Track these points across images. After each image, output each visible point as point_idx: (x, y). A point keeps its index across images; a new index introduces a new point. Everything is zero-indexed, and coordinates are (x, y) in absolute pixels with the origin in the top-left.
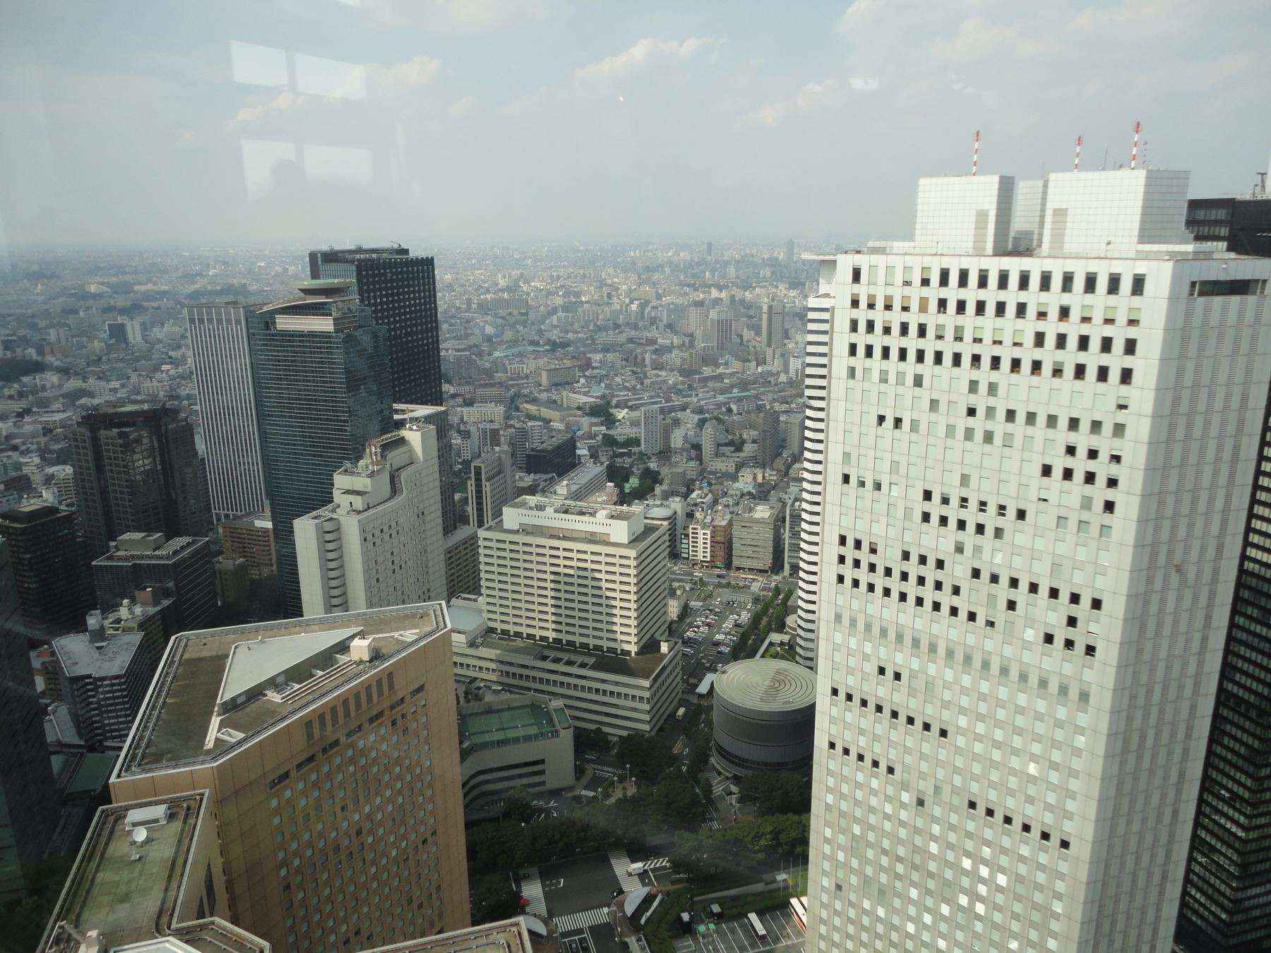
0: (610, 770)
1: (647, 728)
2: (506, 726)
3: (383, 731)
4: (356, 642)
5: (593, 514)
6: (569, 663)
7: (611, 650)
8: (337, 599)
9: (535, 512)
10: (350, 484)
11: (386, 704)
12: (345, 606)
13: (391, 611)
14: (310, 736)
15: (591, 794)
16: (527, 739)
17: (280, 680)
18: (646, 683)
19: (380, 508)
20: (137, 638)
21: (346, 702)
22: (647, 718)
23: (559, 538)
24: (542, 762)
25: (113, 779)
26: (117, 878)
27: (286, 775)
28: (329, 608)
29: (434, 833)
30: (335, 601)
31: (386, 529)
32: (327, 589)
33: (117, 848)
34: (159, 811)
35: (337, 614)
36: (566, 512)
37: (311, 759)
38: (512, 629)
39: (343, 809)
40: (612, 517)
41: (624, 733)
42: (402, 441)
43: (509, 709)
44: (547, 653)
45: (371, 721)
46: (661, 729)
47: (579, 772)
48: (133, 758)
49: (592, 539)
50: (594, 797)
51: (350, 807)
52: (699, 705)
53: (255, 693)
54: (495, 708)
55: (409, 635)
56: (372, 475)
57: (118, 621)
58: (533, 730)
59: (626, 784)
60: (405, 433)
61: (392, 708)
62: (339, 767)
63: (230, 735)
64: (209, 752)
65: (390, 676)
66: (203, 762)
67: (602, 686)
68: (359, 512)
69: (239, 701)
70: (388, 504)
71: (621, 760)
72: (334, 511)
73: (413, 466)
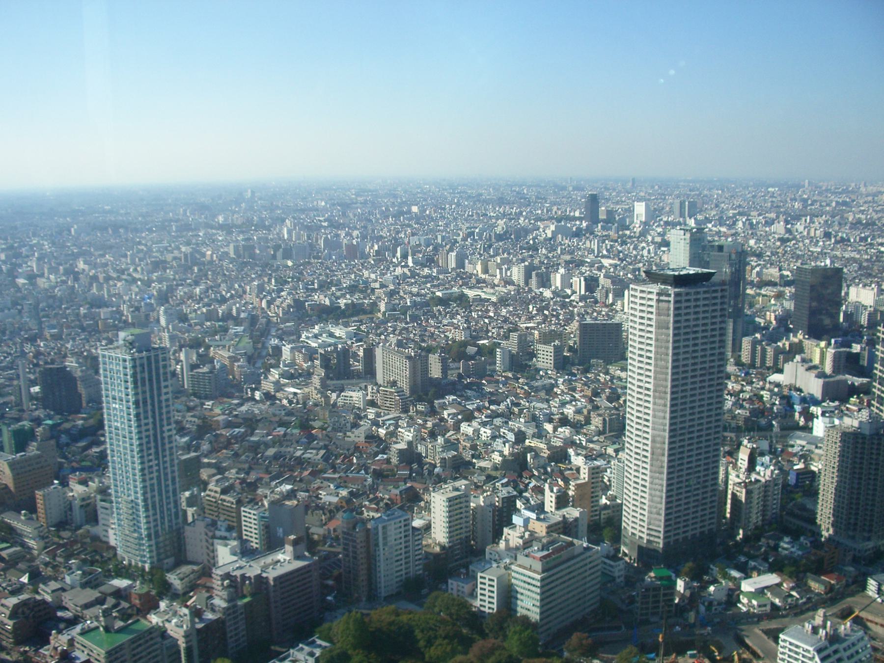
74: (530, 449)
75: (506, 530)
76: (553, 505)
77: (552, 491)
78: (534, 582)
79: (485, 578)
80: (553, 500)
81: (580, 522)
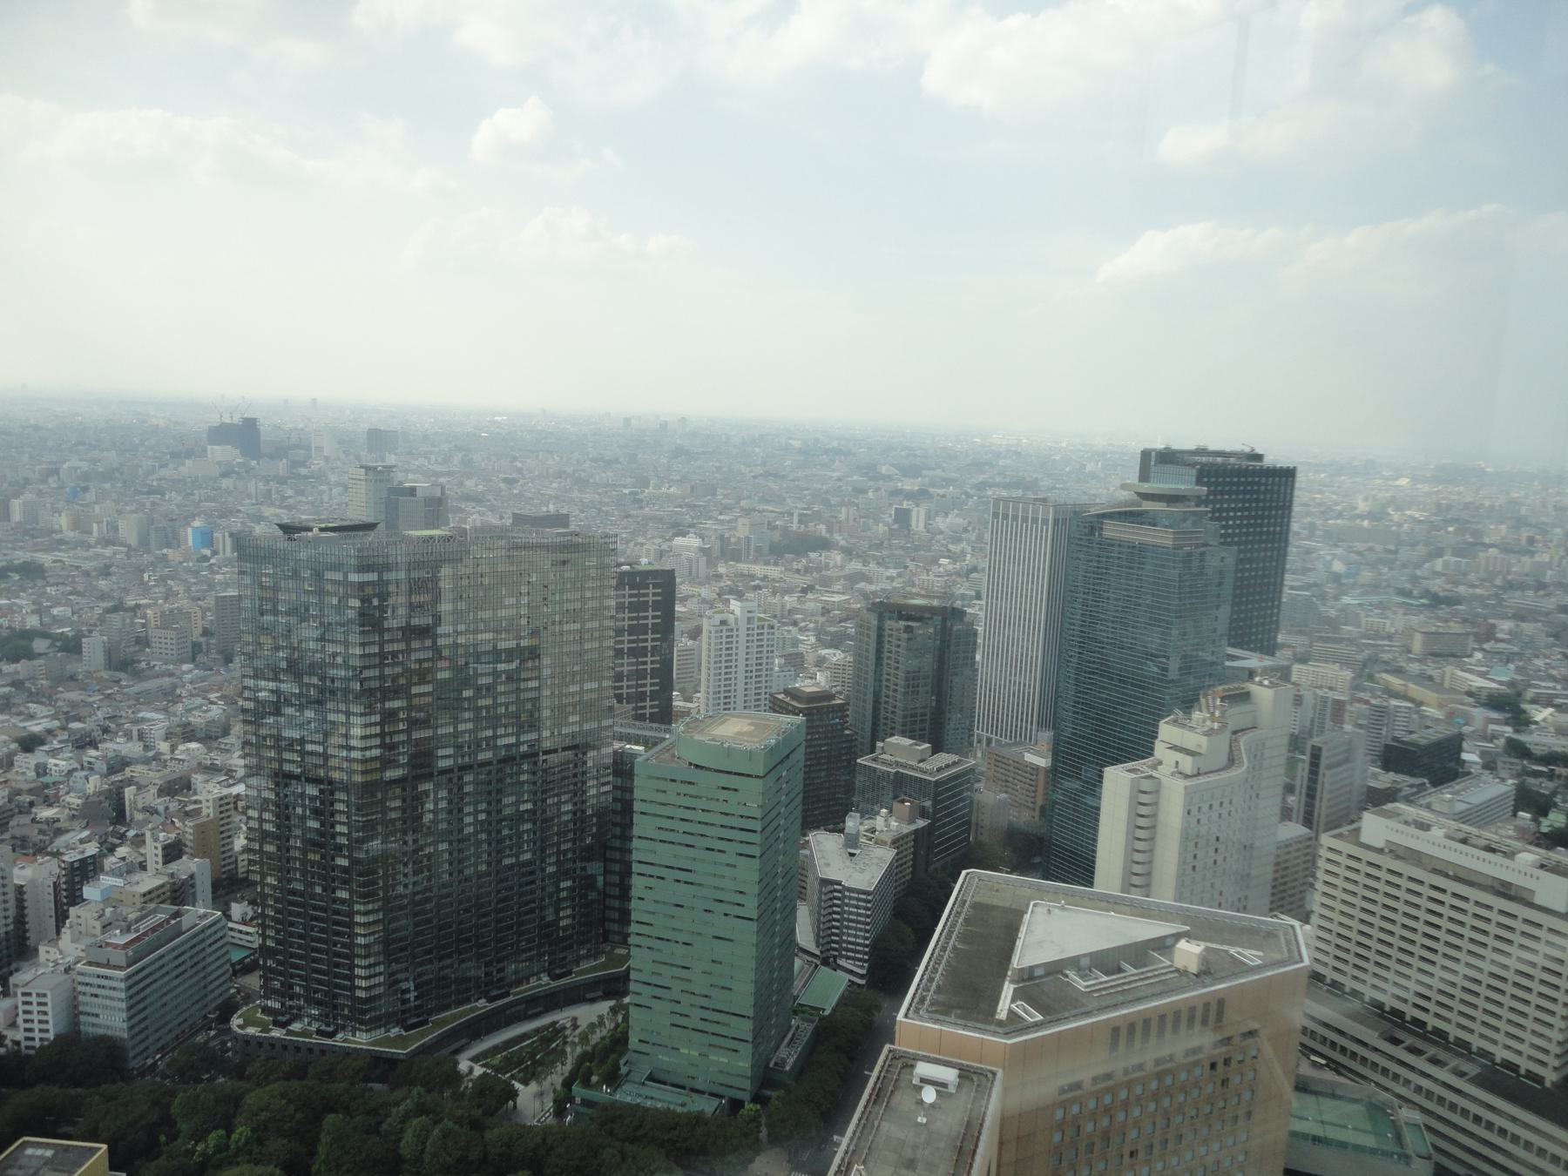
5: (1510, 855)
6: (1435, 1061)
8: (1139, 875)
9: (1412, 830)
10: (1179, 740)
12: (1146, 888)
13: (1224, 916)
16: (1359, 1149)
17: (1085, 962)
19: (1214, 777)
20: (888, 854)
23: (1447, 876)
25: (900, 1017)
28: (1128, 886)
30: (1136, 880)
32: (1130, 862)
33: (902, 1101)
34: (949, 1075)
35: (1136, 896)
36: (1464, 841)
39: (1132, 1154)
40: (1542, 866)
42: (1245, 697)
43: (1333, 1096)
44: (1400, 1034)
48: (922, 1000)
49: (1504, 890)
51: (1141, 1156)
53: (1055, 969)
56: (1207, 734)
57: (873, 831)
58: (1369, 1141)
62: (1138, 1099)
63: (1026, 1012)
64: (1000, 1023)
65: (1221, 1003)
66: (995, 1033)
67: (1487, 1115)
68: (1187, 777)
70: (1224, 775)
73: (1257, 732)
75: (73, 911)
76: (160, 859)
77: (156, 840)
79: (29, 994)
80: (159, 852)
81: (198, 881)
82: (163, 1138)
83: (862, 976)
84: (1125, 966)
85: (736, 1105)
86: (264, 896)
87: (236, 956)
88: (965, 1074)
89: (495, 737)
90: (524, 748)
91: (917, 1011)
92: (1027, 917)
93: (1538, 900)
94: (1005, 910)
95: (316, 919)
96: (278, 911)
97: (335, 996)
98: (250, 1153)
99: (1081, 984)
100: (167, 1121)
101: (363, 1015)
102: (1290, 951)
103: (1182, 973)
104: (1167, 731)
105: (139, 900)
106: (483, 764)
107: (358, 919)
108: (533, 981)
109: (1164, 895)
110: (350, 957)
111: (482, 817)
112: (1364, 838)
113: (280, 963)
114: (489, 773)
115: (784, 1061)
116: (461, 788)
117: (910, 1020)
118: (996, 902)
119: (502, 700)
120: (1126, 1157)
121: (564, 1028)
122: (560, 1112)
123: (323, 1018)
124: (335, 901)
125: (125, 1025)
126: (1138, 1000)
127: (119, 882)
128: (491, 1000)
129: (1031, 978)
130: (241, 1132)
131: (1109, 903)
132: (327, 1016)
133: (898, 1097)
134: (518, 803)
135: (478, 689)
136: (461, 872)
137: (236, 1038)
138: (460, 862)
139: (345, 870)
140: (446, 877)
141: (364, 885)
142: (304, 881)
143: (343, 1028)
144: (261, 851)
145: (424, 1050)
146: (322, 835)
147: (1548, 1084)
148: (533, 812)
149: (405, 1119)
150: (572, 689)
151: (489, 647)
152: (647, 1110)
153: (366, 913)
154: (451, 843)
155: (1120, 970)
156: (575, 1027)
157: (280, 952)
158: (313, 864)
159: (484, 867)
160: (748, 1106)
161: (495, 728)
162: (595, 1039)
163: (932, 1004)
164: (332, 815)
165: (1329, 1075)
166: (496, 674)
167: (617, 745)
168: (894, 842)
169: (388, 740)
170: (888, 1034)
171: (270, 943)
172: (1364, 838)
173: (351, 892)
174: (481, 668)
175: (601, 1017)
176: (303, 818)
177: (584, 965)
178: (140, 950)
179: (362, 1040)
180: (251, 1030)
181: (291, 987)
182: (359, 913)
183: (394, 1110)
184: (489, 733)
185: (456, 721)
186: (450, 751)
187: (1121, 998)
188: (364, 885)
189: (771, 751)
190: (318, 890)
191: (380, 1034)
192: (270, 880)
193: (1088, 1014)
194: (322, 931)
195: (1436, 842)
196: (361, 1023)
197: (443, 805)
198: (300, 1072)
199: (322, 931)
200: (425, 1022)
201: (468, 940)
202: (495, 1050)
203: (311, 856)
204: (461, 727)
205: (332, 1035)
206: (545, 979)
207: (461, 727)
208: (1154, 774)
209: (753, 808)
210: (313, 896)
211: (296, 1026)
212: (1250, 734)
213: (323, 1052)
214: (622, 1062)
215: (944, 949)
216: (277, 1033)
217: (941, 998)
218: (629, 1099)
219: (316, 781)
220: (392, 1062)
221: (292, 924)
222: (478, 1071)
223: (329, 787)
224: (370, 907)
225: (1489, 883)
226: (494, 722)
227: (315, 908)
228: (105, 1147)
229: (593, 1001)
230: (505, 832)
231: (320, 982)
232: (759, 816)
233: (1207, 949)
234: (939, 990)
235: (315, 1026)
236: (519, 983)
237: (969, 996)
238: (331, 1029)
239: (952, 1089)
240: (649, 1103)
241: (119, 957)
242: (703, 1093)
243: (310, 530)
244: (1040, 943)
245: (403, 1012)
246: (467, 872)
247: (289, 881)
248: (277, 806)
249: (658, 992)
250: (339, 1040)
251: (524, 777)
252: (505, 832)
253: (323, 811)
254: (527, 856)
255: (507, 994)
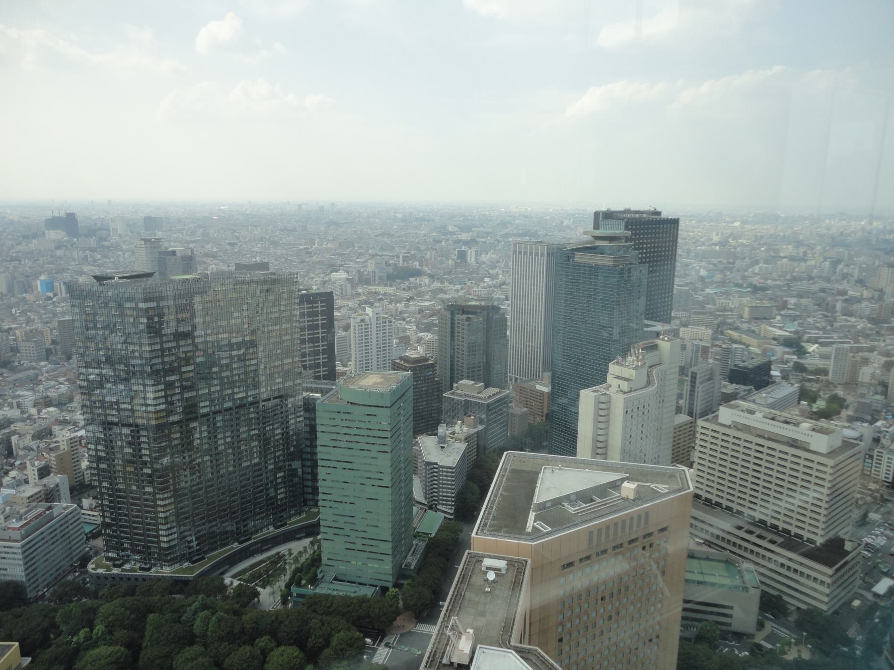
0: (787, 631)
1: (825, 608)
2: (704, 571)
3: (636, 551)
4: (625, 484)
5: (797, 425)
6: (760, 537)
7: (797, 536)
8: (601, 448)
9: (746, 414)
10: (621, 373)
11: (641, 533)
12: (605, 455)
13: (647, 467)
14: (591, 541)
15: (769, 646)
17: (573, 497)
18: (830, 571)
19: (639, 392)
20: (463, 446)
21: (616, 524)
22: (826, 599)
23: (764, 438)
24: (731, 608)
25: (473, 535)
26: (477, 599)
27: (571, 564)
28: (595, 454)
29: (658, 637)
30: (600, 451)
31: (641, 408)
33: (477, 580)
34: (502, 564)
35: (599, 460)
36: (773, 419)
37: (588, 558)
38: (715, 499)
39: (602, 599)
40: (814, 430)
41: (804, 607)
42: (655, 347)
43: (708, 559)
45: (630, 542)
46: (836, 613)
47: (760, 625)
48: (485, 525)
49: (794, 443)
50: (771, 649)
51: (607, 599)
52: (876, 604)
53: (557, 502)
54: (696, 555)
55: (662, 488)
56: (636, 368)
57: (454, 433)
59: (802, 648)
60: (658, 342)
61: (645, 537)
64: (528, 534)
65: (647, 513)
66: (526, 540)
68: (625, 393)
69: (548, 505)
70: (645, 391)
71: (800, 625)
72: (607, 389)
73: (662, 366)
74: (14, 433)
76: (37, 477)
77: (33, 466)
78: (15, 551)
80: (36, 472)
82: (52, 636)
83: (451, 514)
84: (595, 498)
85: (384, 590)
86: (102, 494)
87: (88, 529)
88: (510, 563)
89: (233, 394)
90: (251, 399)
91: (483, 530)
92: (541, 475)
93: (811, 448)
94: (529, 472)
95: (134, 504)
96: (111, 502)
97: (149, 547)
98: (105, 639)
99: (571, 510)
100: (54, 626)
101: (168, 556)
102: (683, 484)
103: (626, 499)
104: (613, 369)
105: (26, 501)
106: (227, 410)
107: (159, 503)
108: (265, 531)
109: (615, 458)
110: (156, 525)
111: (229, 440)
112: (720, 420)
113: (115, 531)
114: (231, 414)
115: (410, 564)
116: (215, 424)
117: (478, 536)
118: (523, 468)
119: (236, 372)
120: (599, 601)
121: (284, 555)
122: (285, 601)
123: (143, 560)
124: (145, 494)
125: (23, 574)
126: (603, 516)
127: (13, 492)
128: (240, 543)
129: (545, 508)
130: (99, 628)
131: (585, 464)
132: (145, 559)
133: (474, 577)
134: (249, 430)
135: (221, 367)
136: (218, 472)
137: (91, 576)
138: (217, 466)
139: (150, 476)
140: (210, 476)
141: (161, 483)
142: (125, 483)
143: (155, 565)
144: (98, 468)
145: (203, 574)
146: (134, 456)
147: (818, 544)
148: (259, 435)
149: (195, 613)
150: (277, 363)
151: (226, 342)
152: (335, 596)
153: (163, 500)
154: (211, 456)
155: (592, 500)
156: (291, 554)
157: (114, 525)
158: (130, 473)
159: (231, 469)
160: (391, 590)
161: (232, 388)
162: (302, 560)
163: (490, 526)
164: (139, 444)
165: (705, 549)
166: (231, 357)
167: (305, 394)
168: (466, 439)
169: (169, 399)
170: (467, 544)
171: (107, 520)
172: (720, 420)
173: (154, 488)
174: (222, 355)
175: (305, 548)
176: (122, 447)
177: (293, 520)
178: (28, 531)
179: (167, 571)
180: (100, 571)
181: (122, 544)
182: (160, 499)
183: (188, 609)
184: (230, 391)
185: (209, 386)
186: (207, 403)
187: (593, 515)
188: (161, 483)
189: (393, 392)
190: (134, 488)
191: (177, 566)
192: (104, 484)
193: (576, 525)
194: (139, 511)
195: (758, 421)
196: (166, 561)
197: (205, 434)
198: (131, 592)
199: (139, 511)
200: (203, 558)
201: (225, 510)
202: (244, 571)
203: (128, 469)
204: (213, 389)
205: (149, 570)
206: (271, 529)
207: (213, 389)
208: (607, 392)
209: (386, 424)
210: (131, 492)
211: (127, 566)
212: (659, 367)
213: (144, 580)
214: (318, 572)
215: (496, 496)
216: (116, 571)
217: (495, 522)
218: (324, 592)
219: (129, 425)
220: (185, 582)
221: (120, 509)
222: (236, 583)
223: (136, 428)
224: (166, 495)
225: (786, 440)
226: (232, 384)
227: (133, 498)
228: (17, 644)
229: (300, 539)
230: (243, 448)
231: (139, 540)
232: (389, 428)
233: (638, 486)
234: (494, 518)
235: (138, 565)
236: (256, 532)
237: (512, 520)
238: (148, 566)
239: (504, 572)
240: (335, 593)
241: (17, 535)
242: (365, 585)
243: (113, 278)
244: (548, 489)
245: (190, 553)
246: (222, 472)
247: (116, 484)
248: (106, 441)
249: (337, 531)
250: (153, 572)
251: (252, 416)
252: (243, 448)
253: (134, 443)
254: (257, 460)
255: (250, 539)
